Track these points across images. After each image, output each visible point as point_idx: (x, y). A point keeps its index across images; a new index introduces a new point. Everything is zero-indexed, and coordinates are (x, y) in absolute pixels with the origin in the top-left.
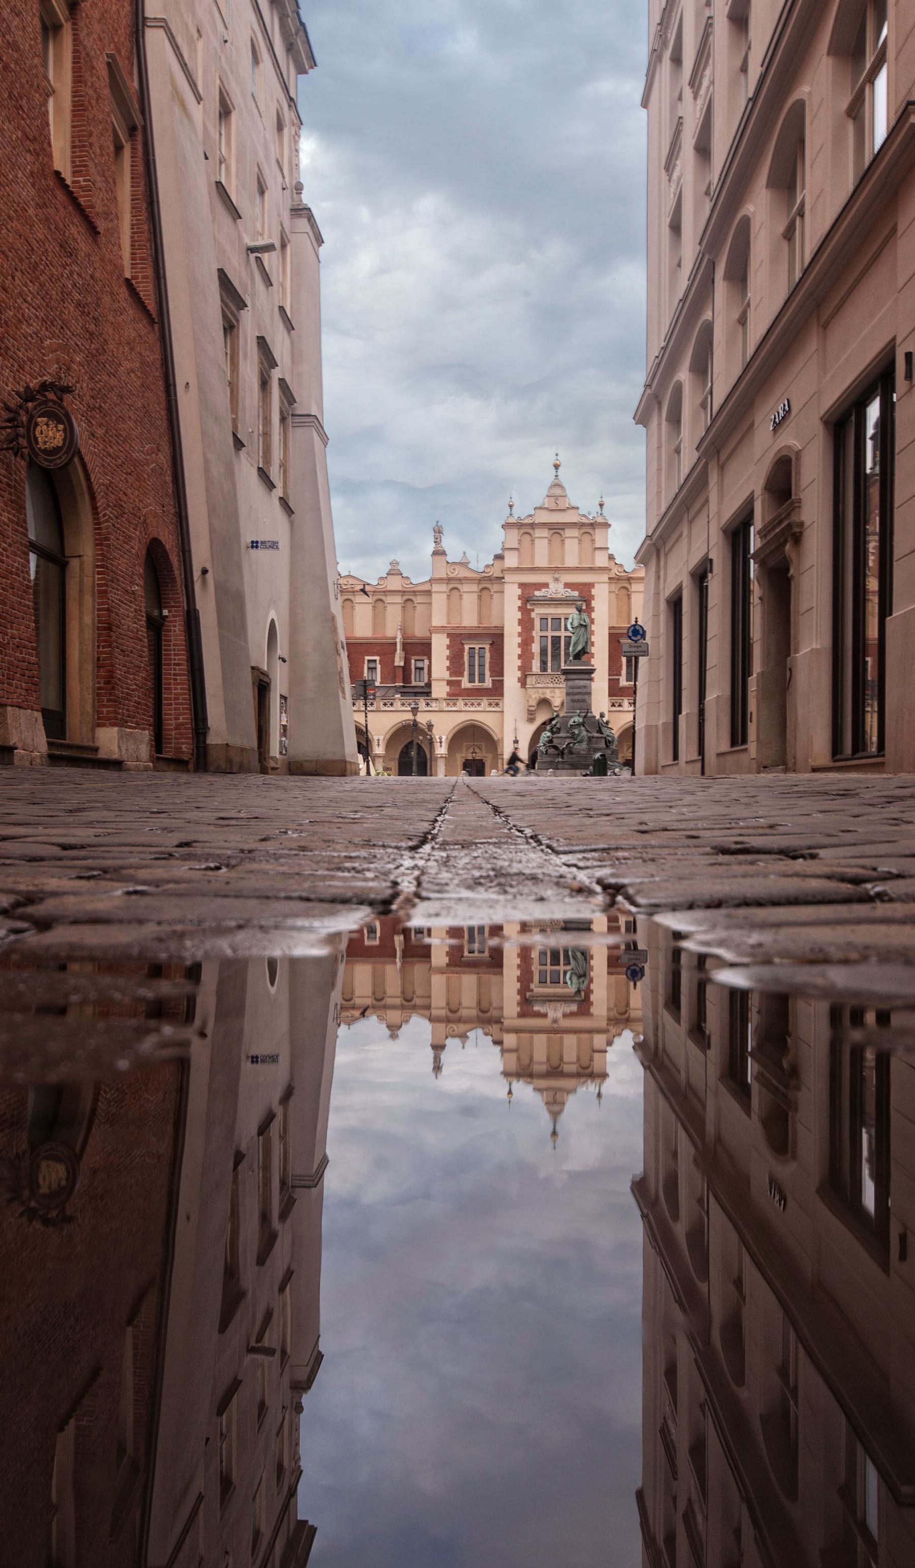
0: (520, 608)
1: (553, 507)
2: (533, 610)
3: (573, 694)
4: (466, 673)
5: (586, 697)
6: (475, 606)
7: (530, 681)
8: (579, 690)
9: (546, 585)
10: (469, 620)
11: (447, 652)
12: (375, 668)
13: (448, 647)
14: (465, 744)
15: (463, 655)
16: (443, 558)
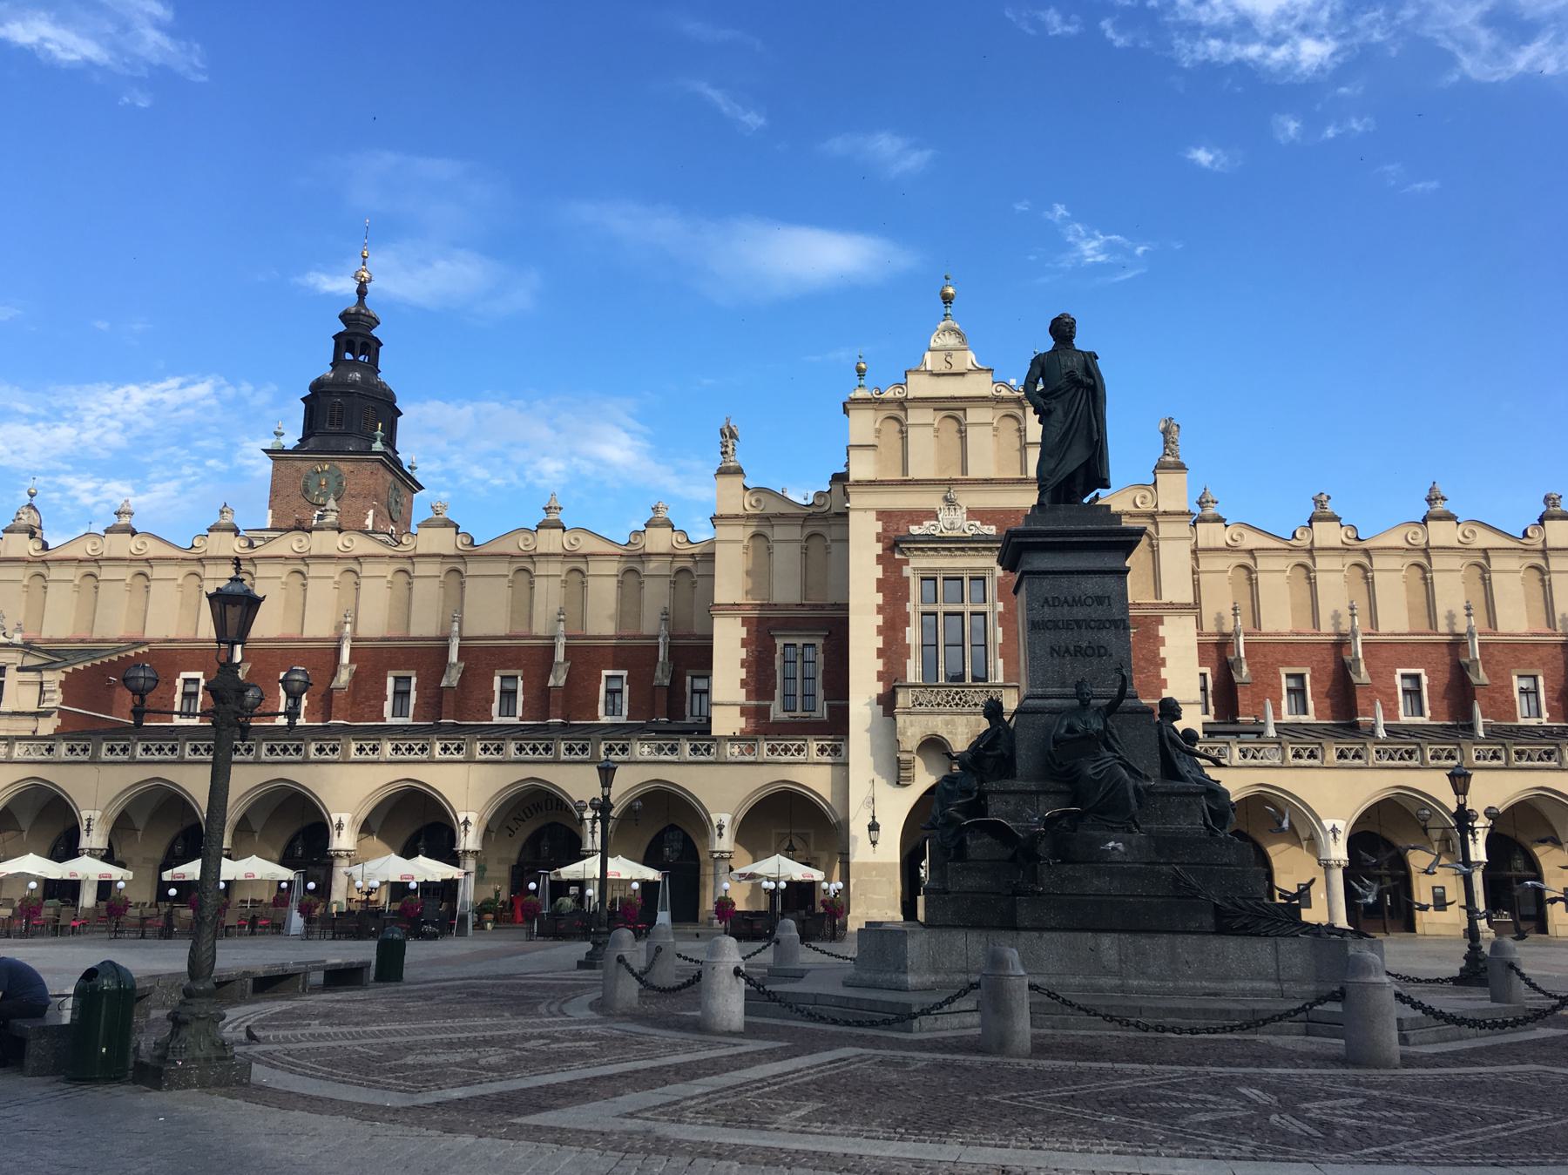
0: (880, 559)
1: (943, 368)
2: (907, 562)
3: (1054, 625)
4: (778, 693)
5: (1107, 637)
6: (797, 567)
7: (904, 699)
8: (1080, 613)
9: (932, 515)
10: (787, 592)
11: (743, 653)
12: (620, 691)
13: (744, 643)
14: (774, 831)
15: (773, 658)
16: (737, 481)
